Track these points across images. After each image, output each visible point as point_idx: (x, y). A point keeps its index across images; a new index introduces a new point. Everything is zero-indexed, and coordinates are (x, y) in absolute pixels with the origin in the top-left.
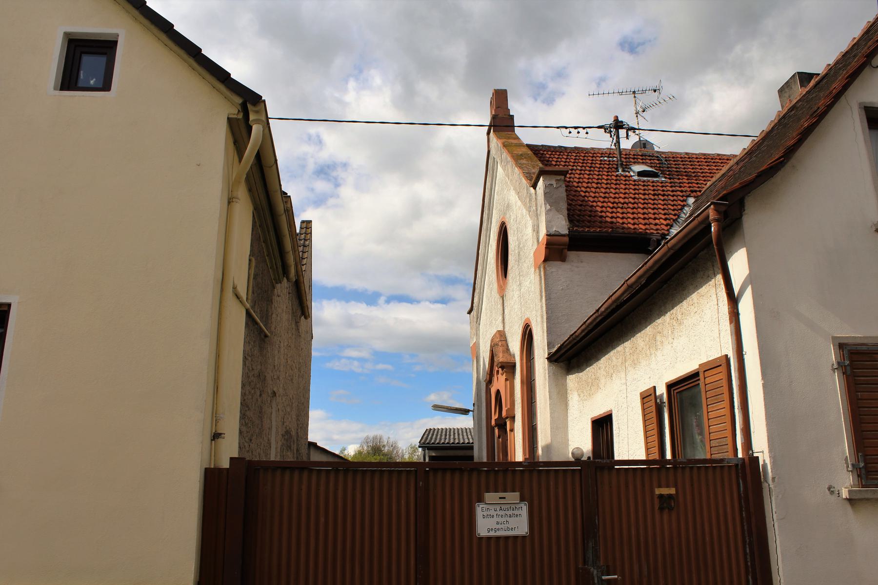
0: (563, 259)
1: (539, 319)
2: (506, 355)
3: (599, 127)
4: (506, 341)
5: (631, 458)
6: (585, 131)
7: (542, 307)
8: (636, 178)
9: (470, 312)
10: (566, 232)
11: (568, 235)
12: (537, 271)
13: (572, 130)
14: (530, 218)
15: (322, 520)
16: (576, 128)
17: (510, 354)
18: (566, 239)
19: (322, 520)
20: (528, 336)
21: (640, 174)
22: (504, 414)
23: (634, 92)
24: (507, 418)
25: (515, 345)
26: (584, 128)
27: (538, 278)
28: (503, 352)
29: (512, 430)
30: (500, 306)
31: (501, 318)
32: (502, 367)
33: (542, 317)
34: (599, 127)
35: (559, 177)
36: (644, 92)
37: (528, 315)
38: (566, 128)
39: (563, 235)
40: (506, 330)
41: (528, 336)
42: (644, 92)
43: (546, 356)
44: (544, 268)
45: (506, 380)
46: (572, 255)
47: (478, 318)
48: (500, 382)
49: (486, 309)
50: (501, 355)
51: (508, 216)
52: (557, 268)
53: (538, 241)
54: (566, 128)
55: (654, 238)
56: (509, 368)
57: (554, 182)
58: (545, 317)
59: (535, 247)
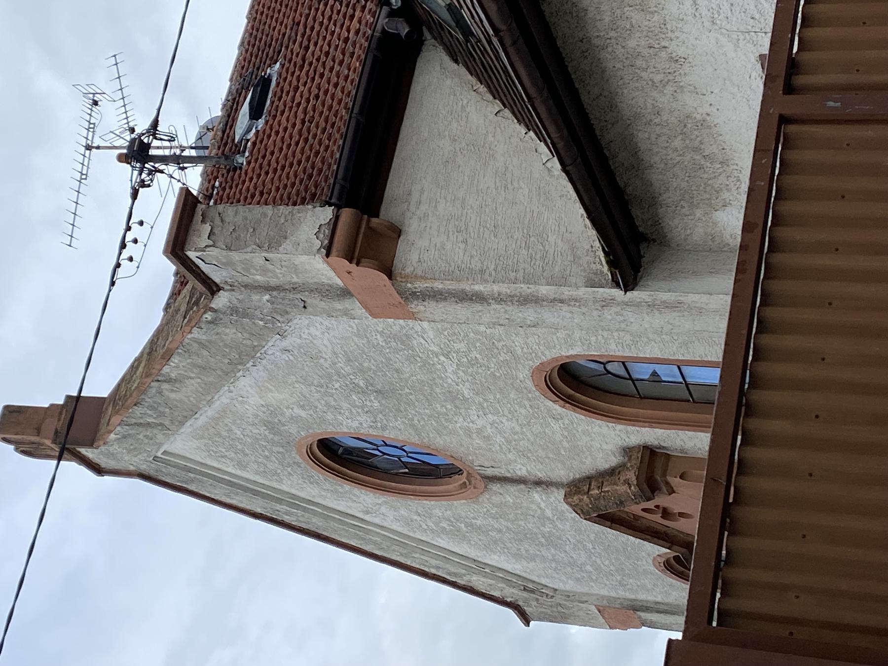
1: (529, 314)
3: (135, 195)
4: (589, 479)
6: (135, 227)
7: (500, 299)
8: (261, 123)
9: (526, 619)
10: (328, 213)
11: (338, 207)
12: (416, 306)
13: (126, 254)
16: (123, 246)
18: (347, 214)
20: (577, 384)
21: (255, 114)
23: (89, 148)
25: (601, 441)
26: (129, 228)
30: (509, 495)
31: (537, 496)
33: (525, 300)
34: (135, 195)
35: (198, 217)
36: (92, 127)
37: (523, 374)
38: (118, 265)
39: (337, 218)
40: (563, 474)
41: (577, 384)
42: (92, 127)
43: (618, 293)
46: (389, 211)
49: (517, 556)
50: (622, 489)
51: (293, 429)
52: (416, 252)
53: (345, 293)
54: (118, 265)
55: (383, 21)
57: (207, 228)
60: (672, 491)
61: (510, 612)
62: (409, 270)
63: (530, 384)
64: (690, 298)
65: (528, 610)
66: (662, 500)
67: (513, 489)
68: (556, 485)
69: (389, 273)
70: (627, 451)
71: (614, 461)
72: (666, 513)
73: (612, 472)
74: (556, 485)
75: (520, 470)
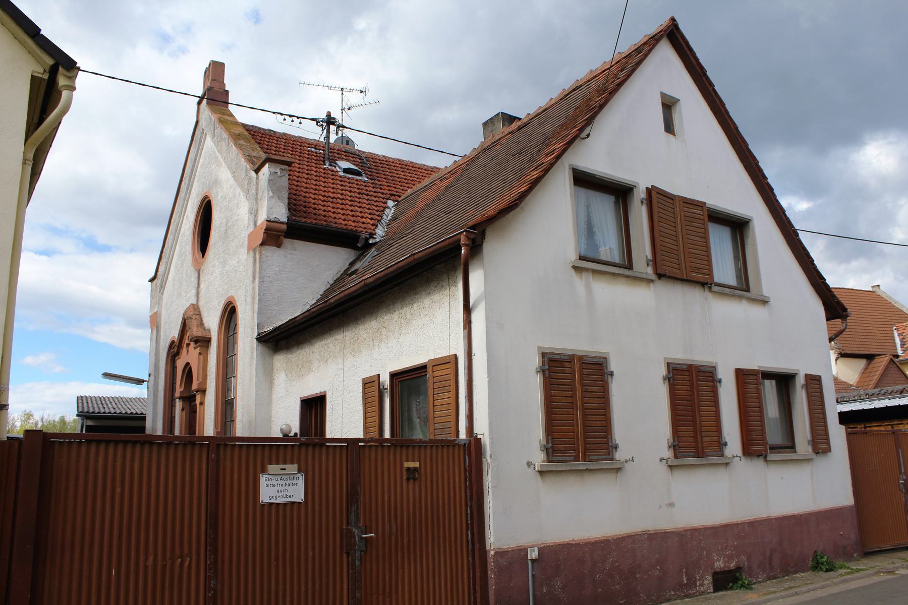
0: (279, 245)
1: (249, 300)
2: (200, 329)
3: (312, 119)
4: (200, 314)
5: (344, 437)
6: (299, 120)
7: (254, 288)
8: (341, 174)
9: (151, 280)
10: (285, 220)
11: (287, 223)
12: (251, 253)
13: (287, 117)
14: (247, 202)
15: (118, 490)
16: (290, 116)
17: (204, 329)
18: (285, 227)
19: (118, 490)
20: (230, 313)
21: (346, 171)
22: (195, 386)
23: (342, 89)
24: (197, 391)
25: (212, 321)
26: (298, 118)
27: (251, 260)
28: (198, 326)
29: (202, 404)
30: (194, 279)
31: (194, 291)
32: (196, 341)
33: (253, 298)
34: (312, 119)
35: (284, 167)
36: (351, 90)
37: (232, 293)
38: (282, 114)
39: (282, 223)
40: (201, 304)
41: (230, 313)
42: (351, 90)
43: (255, 335)
44: (260, 252)
45: (200, 353)
46: (287, 242)
47: (163, 287)
48: (190, 355)
49: (173, 280)
50: (195, 329)
51: (214, 191)
52: (271, 253)
53: (255, 224)
54: (282, 114)
55: (363, 236)
56: (204, 342)
57: (278, 171)
58: (257, 298)
59: (251, 229)
60: (195, 348)
61: (153, 275)
62: (263, 252)
63: (229, 295)
64: (255, 363)
65: (155, 282)
66: (192, 344)
67: (196, 282)
68: (198, 300)
69: (262, 244)
70: (209, 331)
71: (206, 325)
72: (188, 345)
73: (201, 324)
74: (198, 300)
75: (202, 286)
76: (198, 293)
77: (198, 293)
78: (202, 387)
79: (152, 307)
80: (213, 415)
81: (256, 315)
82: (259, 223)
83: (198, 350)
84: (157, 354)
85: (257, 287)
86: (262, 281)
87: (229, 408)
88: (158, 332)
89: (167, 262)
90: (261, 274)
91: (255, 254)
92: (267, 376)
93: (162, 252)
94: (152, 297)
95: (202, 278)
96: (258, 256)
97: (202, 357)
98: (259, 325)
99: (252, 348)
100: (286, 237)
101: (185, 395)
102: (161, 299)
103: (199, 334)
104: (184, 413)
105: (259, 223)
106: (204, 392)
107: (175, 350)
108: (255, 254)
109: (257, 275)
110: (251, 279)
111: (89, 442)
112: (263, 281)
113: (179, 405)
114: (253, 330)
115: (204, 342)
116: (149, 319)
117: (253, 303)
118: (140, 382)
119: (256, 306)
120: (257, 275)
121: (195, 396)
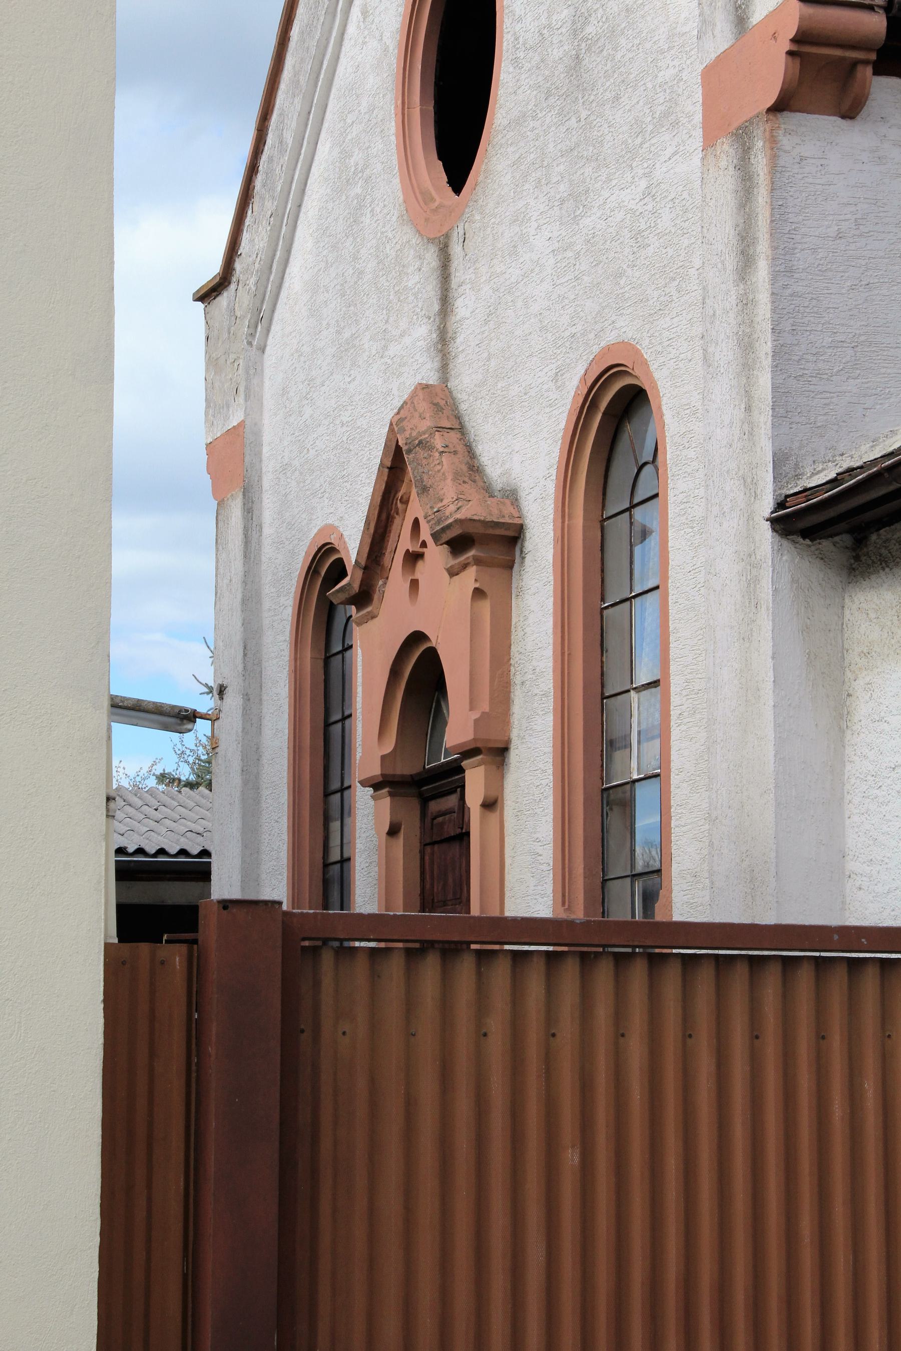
0: (850, 109)
1: (725, 353)
2: (470, 490)
4: (461, 429)
7: (746, 303)
12: (726, 149)
15: (571, 1157)
17: (488, 490)
19: (571, 1157)
22: (458, 730)
24: (471, 752)
25: (525, 455)
27: (725, 181)
28: (457, 476)
29: (491, 805)
31: (423, 333)
32: (460, 542)
33: (746, 345)
37: (623, 329)
40: (465, 382)
43: (766, 505)
44: (773, 141)
45: (478, 593)
47: (261, 318)
48: (431, 600)
50: (448, 490)
53: (741, 20)
56: (490, 544)
58: (765, 347)
59: (721, 39)
60: (453, 573)
61: (213, 268)
62: (786, 142)
63: (611, 337)
64: (765, 624)
65: (224, 300)
66: (437, 557)
67: (431, 291)
68: (444, 369)
69: (780, 107)
70: (512, 496)
71: (494, 472)
72: (413, 558)
73: (473, 469)
74: (444, 369)
75: (465, 306)
76: (443, 341)
77: (443, 341)
78: (494, 737)
79: (214, 406)
80: (547, 853)
81: (764, 419)
82: (758, 14)
83: (469, 579)
84: (250, 600)
85: (764, 298)
86: (783, 271)
87: (615, 820)
88: (250, 510)
89: (278, 216)
90: (772, 237)
91: (745, 153)
92: (825, 681)
93: (252, 169)
94: (212, 363)
95: (460, 273)
96: (760, 163)
97: (485, 607)
98: (779, 461)
99: (749, 560)
100: (880, 70)
101: (406, 768)
102: (255, 370)
103: (474, 509)
104: (399, 843)
105: (758, 14)
106: (500, 753)
107: (333, 590)
108: (745, 153)
109: (763, 247)
110: (731, 262)
111: (416, 953)
112: (790, 271)
113: (368, 816)
114: (751, 487)
115: (490, 544)
116: (202, 457)
117: (747, 367)
118: (181, 718)
119: (764, 381)
120: (763, 247)
121: (455, 770)
